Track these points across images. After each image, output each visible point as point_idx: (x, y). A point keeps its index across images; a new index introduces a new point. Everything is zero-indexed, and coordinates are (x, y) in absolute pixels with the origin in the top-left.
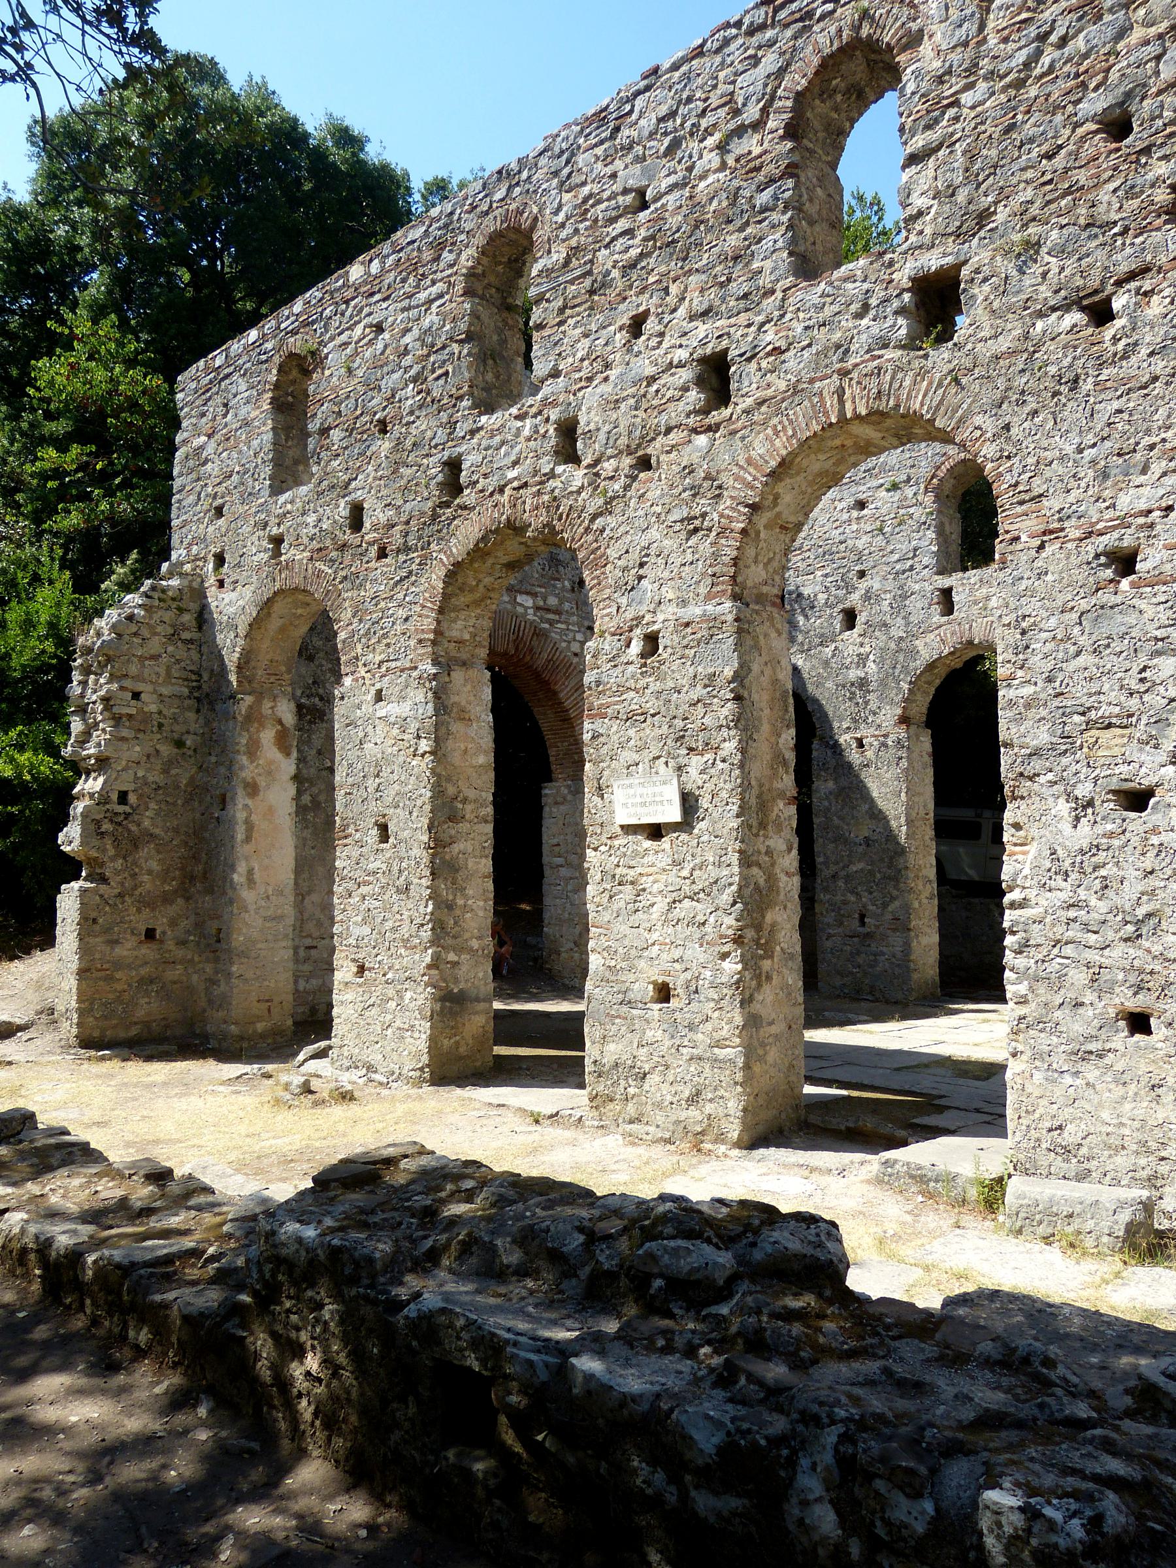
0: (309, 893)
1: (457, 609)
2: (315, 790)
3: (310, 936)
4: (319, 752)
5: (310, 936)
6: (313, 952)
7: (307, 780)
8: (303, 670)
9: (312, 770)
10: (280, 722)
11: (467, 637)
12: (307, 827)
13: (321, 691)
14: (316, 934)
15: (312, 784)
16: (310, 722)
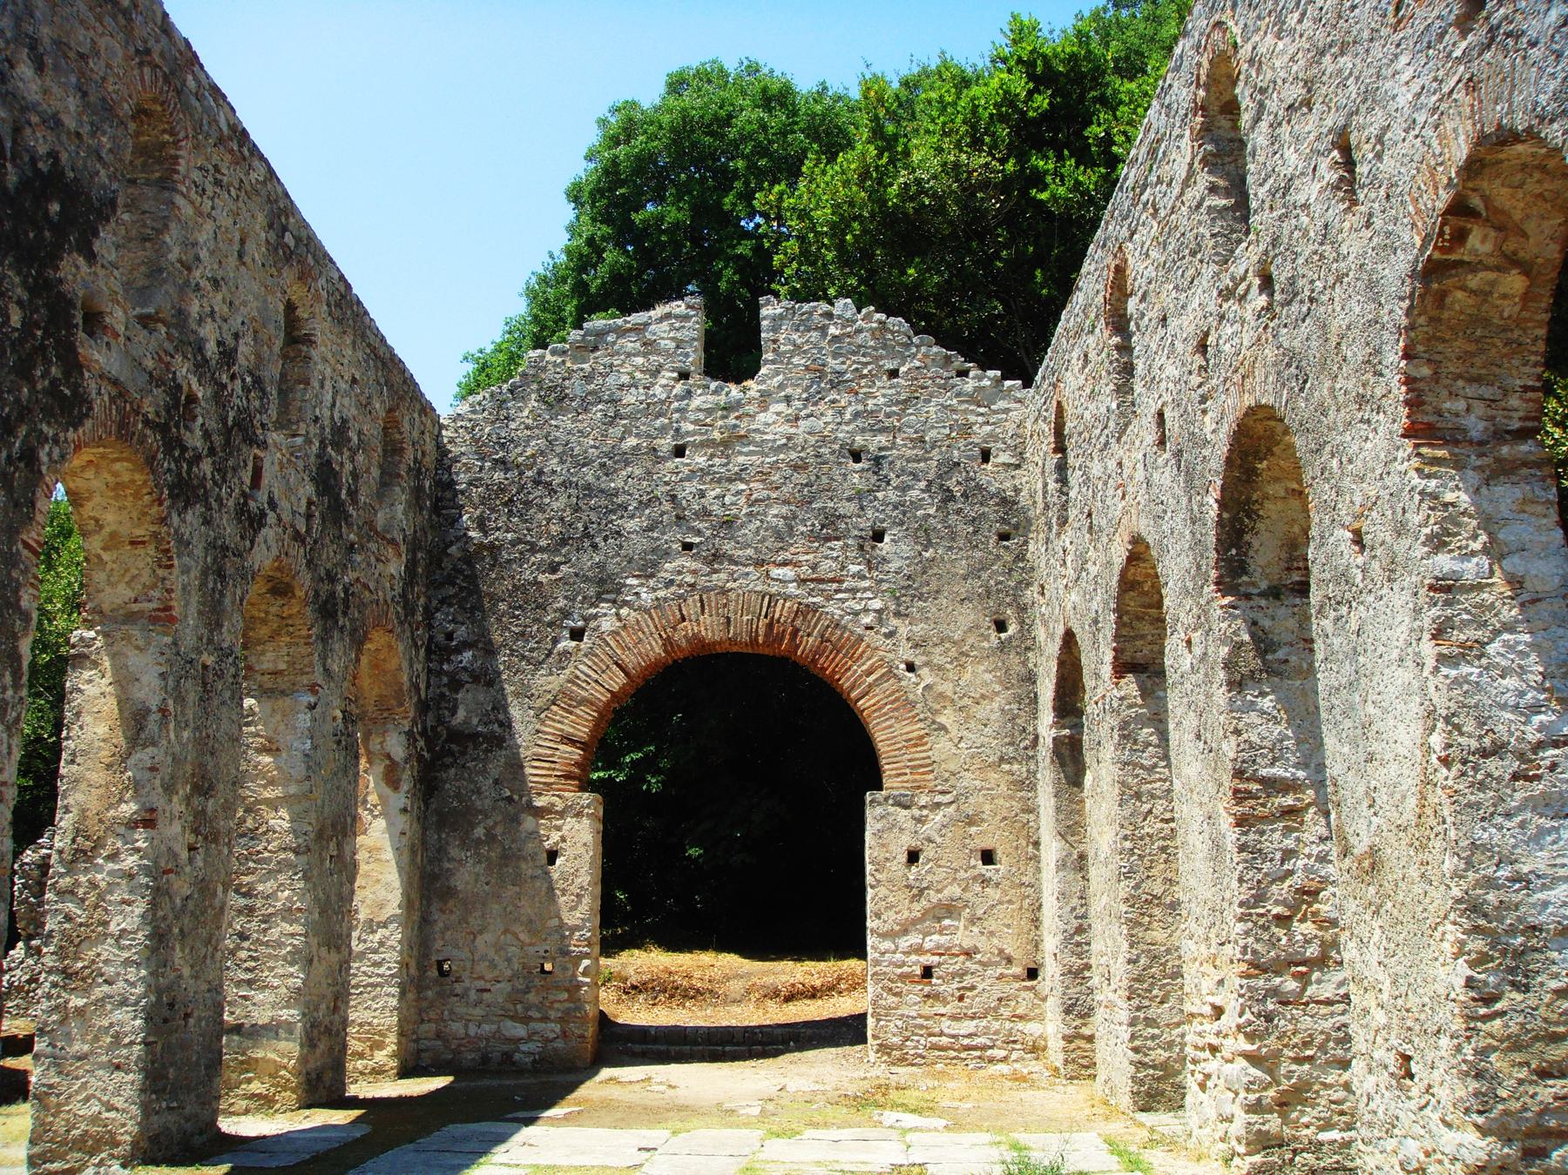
0: (481, 932)
1: (260, 642)
2: (490, 822)
3: (481, 978)
4: (496, 782)
5: (481, 978)
6: (486, 996)
7: (480, 812)
8: (481, 697)
9: (487, 801)
10: (388, 756)
11: (282, 666)
12: (479, 862)
13: (501, 717)
14: (489, 976)
15: (487, 817)
16: (487, 751)
